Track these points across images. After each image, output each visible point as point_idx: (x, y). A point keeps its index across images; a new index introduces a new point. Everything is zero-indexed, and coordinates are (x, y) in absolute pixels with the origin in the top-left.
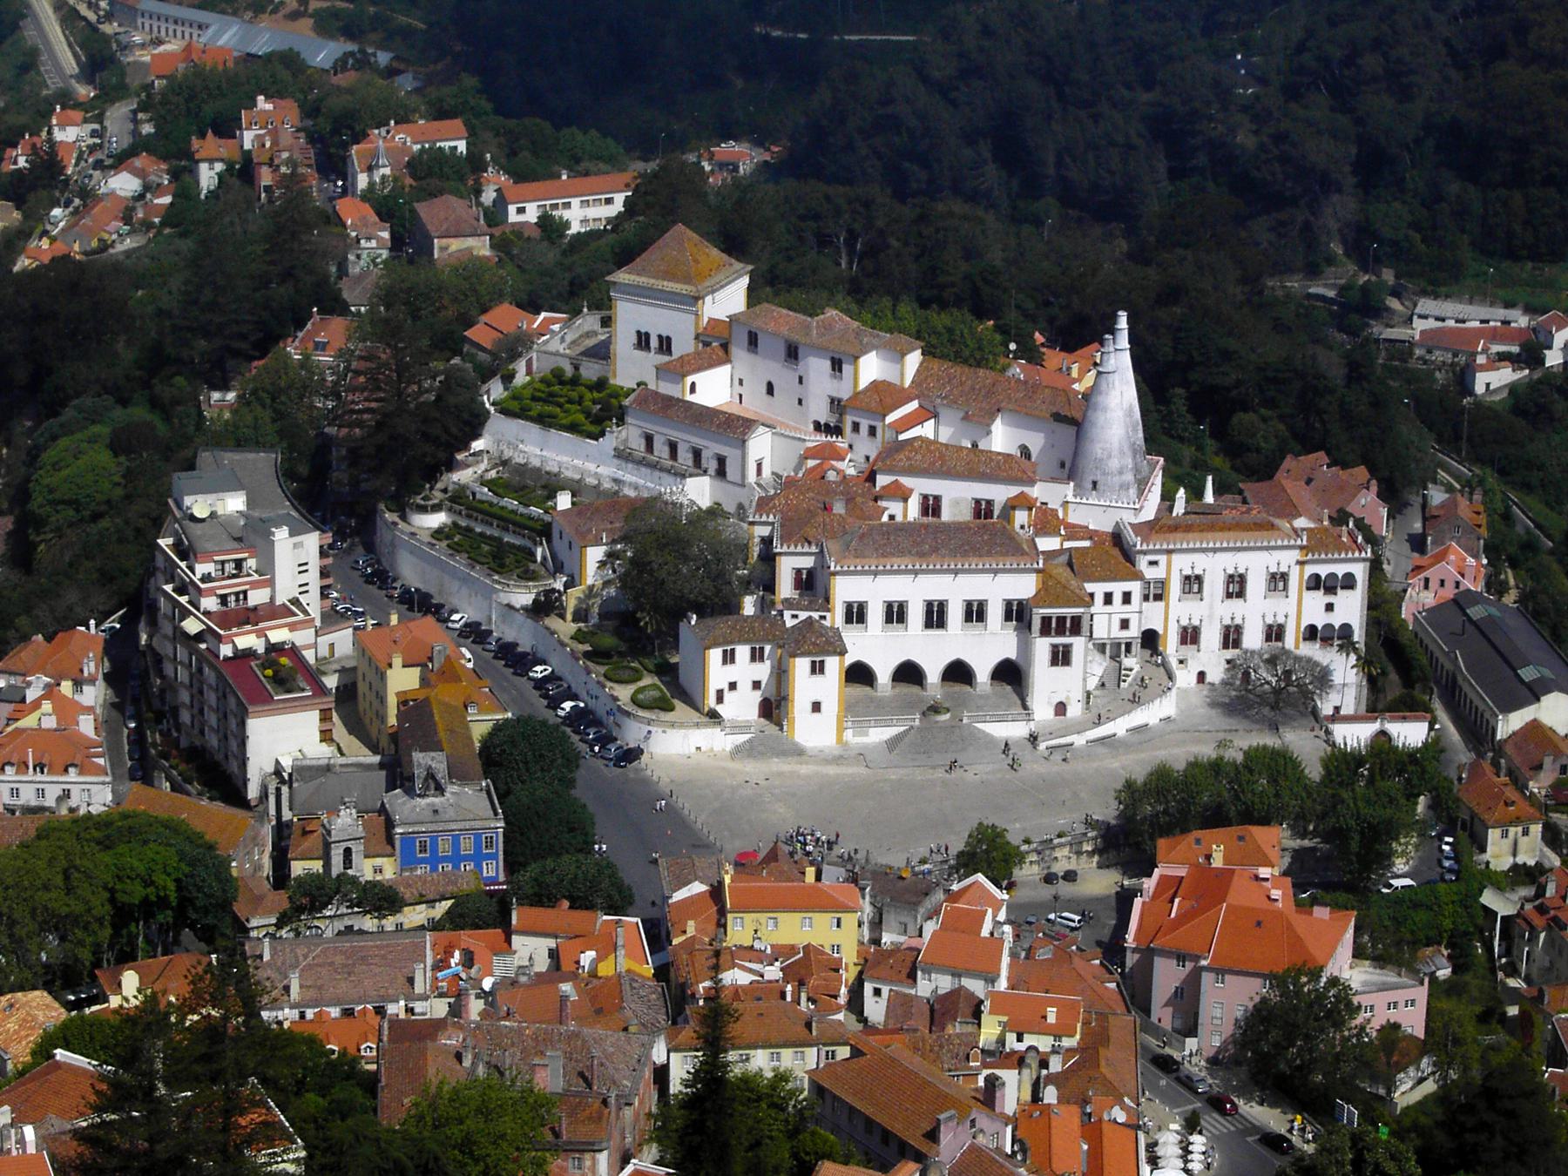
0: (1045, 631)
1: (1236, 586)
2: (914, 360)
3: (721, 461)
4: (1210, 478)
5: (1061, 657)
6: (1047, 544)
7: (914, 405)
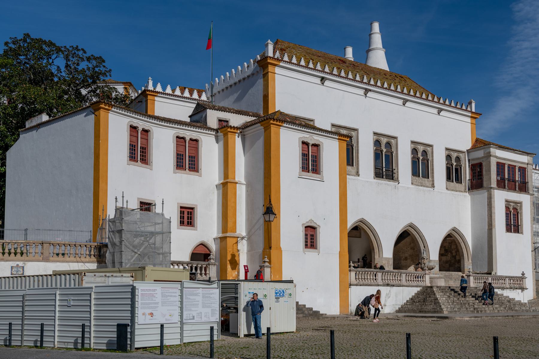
0: (501, 185)
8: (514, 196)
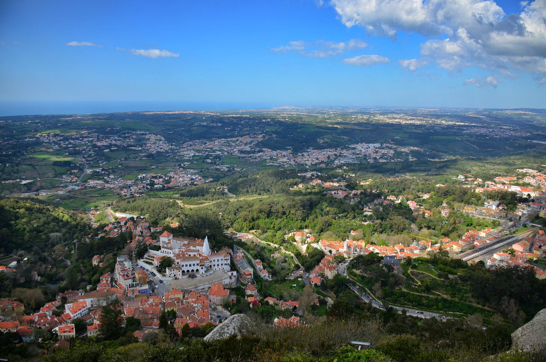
1: (218, 261)
5: (202, 268)
6: (201, 258)
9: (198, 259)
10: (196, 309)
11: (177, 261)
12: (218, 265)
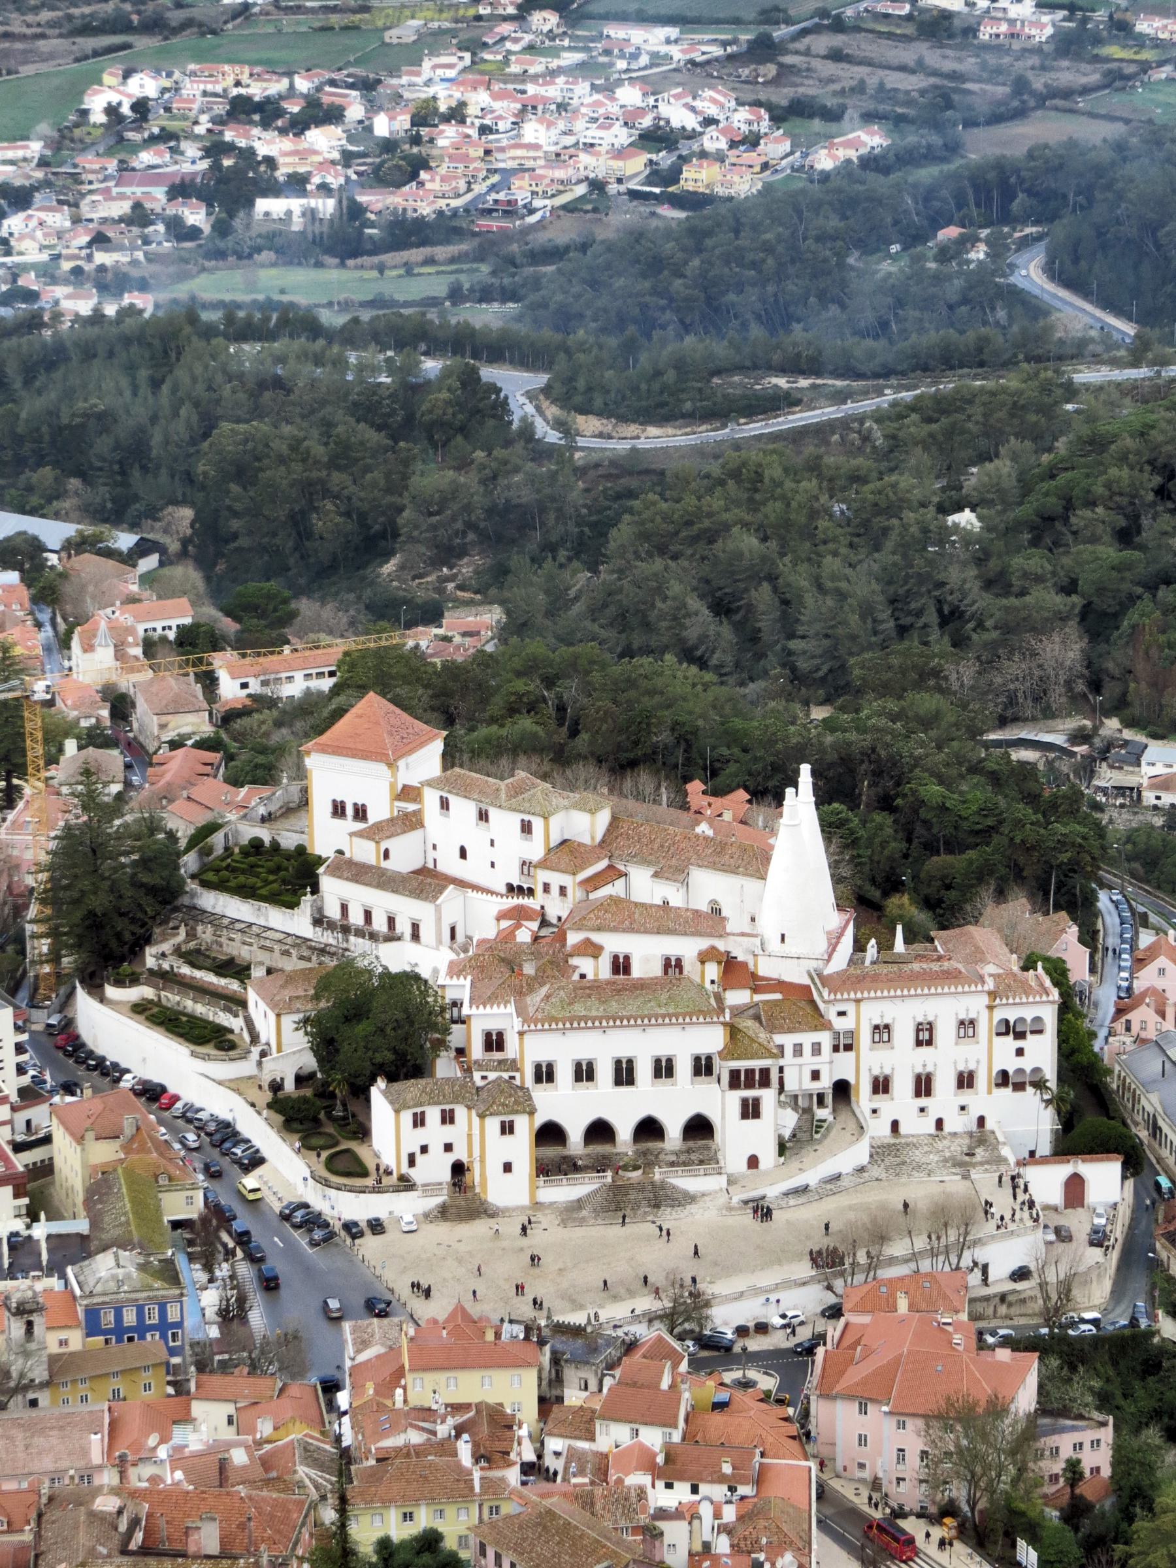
1: (925, 1036)
2: (604, 818)
3: (415, 927)
4: (899, 928)
5: (751, 1110)
7: (603, 864)
8: (750, 1093)
9: (707, 1009)
10: (675, 1532)
11: (484, 1018)
12: (923, 1086)
